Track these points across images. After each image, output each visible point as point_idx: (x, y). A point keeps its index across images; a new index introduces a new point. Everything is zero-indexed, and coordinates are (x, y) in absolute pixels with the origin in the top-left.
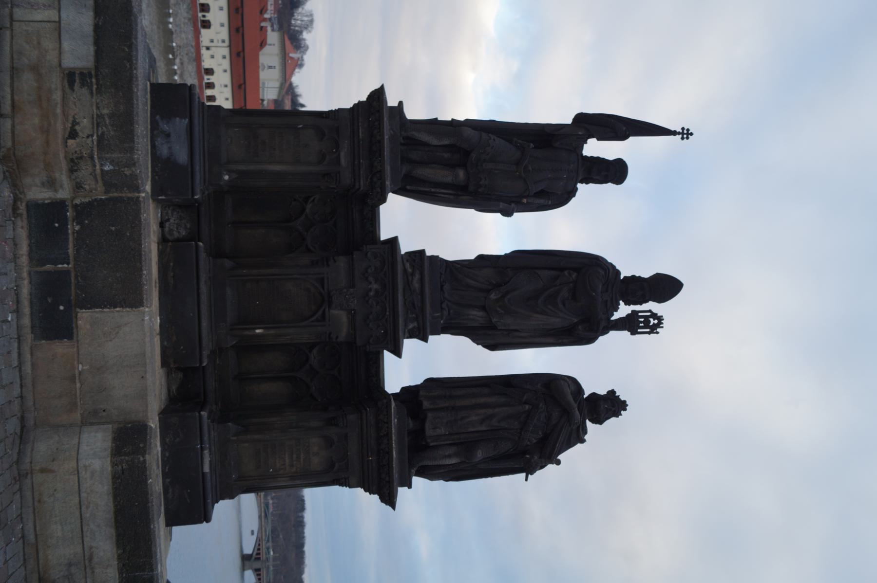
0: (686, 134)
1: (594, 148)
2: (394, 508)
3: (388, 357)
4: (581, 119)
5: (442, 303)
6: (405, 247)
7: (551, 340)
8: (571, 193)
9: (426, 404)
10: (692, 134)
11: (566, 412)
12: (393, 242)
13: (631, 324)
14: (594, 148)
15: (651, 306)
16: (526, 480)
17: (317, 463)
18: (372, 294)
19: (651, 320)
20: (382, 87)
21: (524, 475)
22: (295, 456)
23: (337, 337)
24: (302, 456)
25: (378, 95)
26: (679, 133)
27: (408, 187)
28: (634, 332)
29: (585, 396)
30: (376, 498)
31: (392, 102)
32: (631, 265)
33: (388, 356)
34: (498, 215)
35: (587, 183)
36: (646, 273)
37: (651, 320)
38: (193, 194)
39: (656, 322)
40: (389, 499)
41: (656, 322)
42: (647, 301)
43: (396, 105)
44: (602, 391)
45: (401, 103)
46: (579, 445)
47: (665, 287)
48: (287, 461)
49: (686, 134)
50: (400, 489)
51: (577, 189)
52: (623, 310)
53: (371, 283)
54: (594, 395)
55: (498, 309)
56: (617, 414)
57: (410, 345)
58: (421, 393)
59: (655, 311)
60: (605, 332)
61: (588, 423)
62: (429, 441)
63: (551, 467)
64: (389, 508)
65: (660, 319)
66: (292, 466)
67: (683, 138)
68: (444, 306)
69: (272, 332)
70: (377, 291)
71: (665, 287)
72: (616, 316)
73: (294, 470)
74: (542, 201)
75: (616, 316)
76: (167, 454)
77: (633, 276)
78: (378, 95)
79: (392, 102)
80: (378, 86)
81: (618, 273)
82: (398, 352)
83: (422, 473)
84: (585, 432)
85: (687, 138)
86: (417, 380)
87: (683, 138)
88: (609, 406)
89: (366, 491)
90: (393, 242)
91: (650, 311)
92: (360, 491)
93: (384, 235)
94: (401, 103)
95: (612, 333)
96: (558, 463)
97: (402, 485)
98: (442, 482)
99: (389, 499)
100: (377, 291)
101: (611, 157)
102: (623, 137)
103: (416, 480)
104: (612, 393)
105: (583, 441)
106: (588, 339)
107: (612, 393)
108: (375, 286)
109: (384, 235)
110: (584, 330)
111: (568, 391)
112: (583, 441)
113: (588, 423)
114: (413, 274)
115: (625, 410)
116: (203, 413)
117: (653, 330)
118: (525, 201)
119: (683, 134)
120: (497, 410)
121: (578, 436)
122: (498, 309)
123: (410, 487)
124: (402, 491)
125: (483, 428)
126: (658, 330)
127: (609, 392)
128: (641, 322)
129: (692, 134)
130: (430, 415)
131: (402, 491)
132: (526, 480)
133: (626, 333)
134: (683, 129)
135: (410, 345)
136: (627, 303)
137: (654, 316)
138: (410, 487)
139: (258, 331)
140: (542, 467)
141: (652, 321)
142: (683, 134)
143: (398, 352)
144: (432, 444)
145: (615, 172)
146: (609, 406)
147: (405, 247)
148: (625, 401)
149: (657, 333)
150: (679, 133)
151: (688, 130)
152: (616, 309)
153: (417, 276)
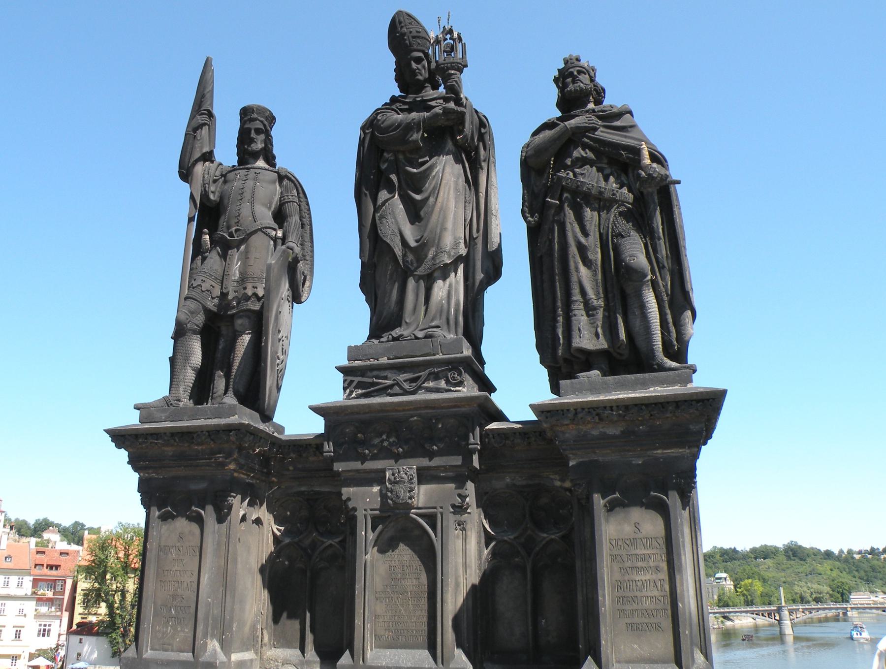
4: (185, 174)
5: (416, 338)
11: (574, 138)
14: (226, 153)
16: (679, 182)
17: (650, 524)
24: (639, 552)
31: (131, 419)
43: (137, 413)
45: (137, 407)
48: (648, 577)
54: (559, 105)
68: (420, 334)
77: (397, 79)
83: (677, 350)
115: (578, 60)
122: (430, 256)
124: (701, 382)
132: (679, 182)
147: (334, 392)
148: (566, 62)
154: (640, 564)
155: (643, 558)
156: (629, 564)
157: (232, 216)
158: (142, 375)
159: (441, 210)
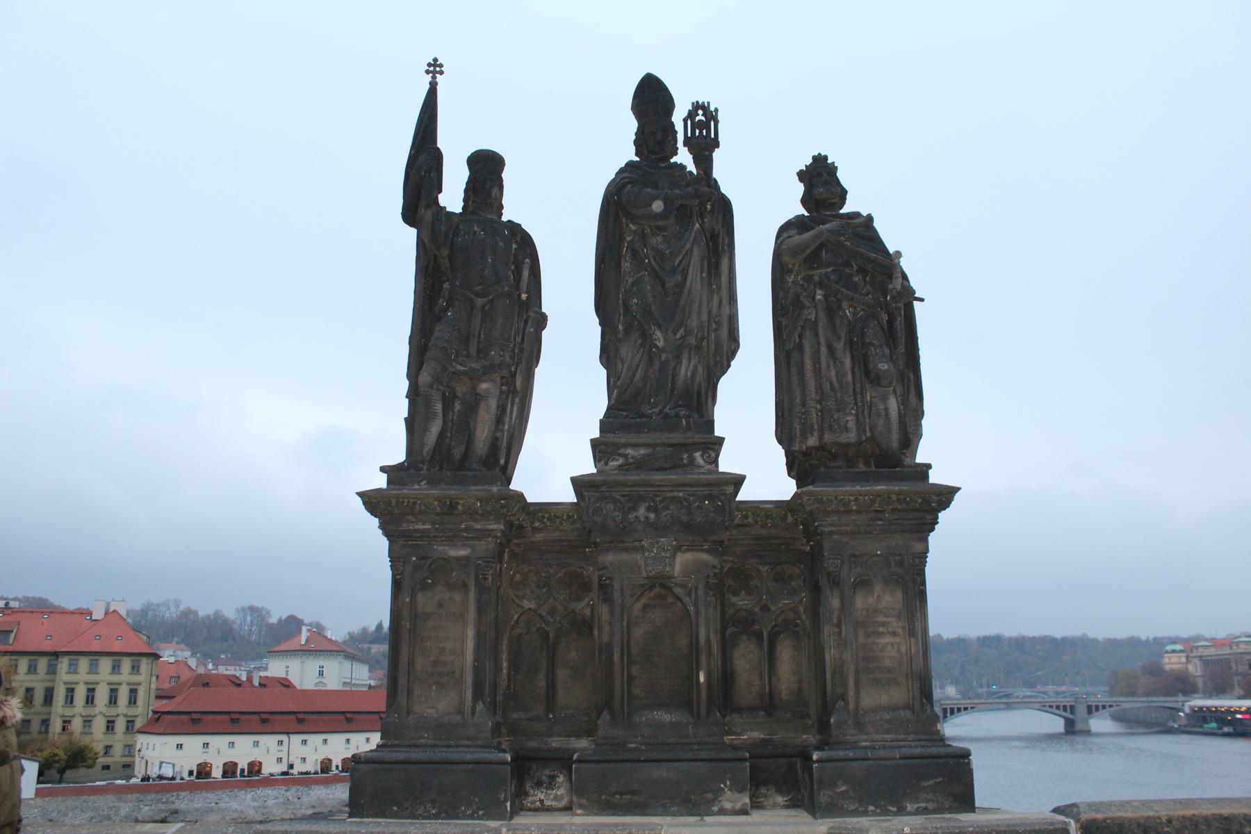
0: (435, 68)
1: (452, 197)
2: (959, 489)
3: (744, 495)
4: (410, 216)
6: (587, 466)
7: (725, 262)
8: (515, 228)
9: (812, 441)
10: (435, 60)
12: (579, 484)
13: (704, 146)
14: (452, 197)
15: (678, 118)
16: (922, 300)
18: (652, 516)
19: (698, 118)
20: (361, 494)
21: (915, 303)
22: (881, 629)
23: (714, 567)
25: (371, 501)
26: (434, 78)
27: (502, 462)
28: (716, 143)
29: (806, 214)
30: (943, 516)
31: (381, 481)
32: (618, 146)
33: (744, 495)
34: (545, 334)
35: (502, 207)
36: (631, 125)
37: (698, 118)
38: (506, 763)
39: (700, 112)
40: (946, 495)
41: (700, 112)
42: (672, 125)
44: (800, 188)
45: (383, 469)
46: (875, 224)
47: (651, 98)
49: (435, 68)
50: (931, 481)
51: (509, 221)
52: (684, 157)
53: (637, 517)
54: (804, 201)
55: (678, 336)
56: (832, 170)
57: (727, 463)
58: (796, 447)
59: (686, 114)
60: (714, 185)
61: (844, 211)
62: (864, 438)
63: (904, 263)
64: (957, 497)
65: (697, 106)
66: (894, 634)
67: (442, 73)
69: (703, 658)
70: (649, 509)
71: (651, 98)
72: (691, 167)
73: (900, 631)
74: (526, 273)
75: (691, 167)
76: (871, 808)
77: (636, 143)
78: (371, 501)
79: (381, 481)
80: (359, 501)
81: (630, 164)
82: (738, 481)
84: (858, 214)
85: (441, 66)
86: (778, 455)
87: (442, 73)
88: (820, 180)
89: (933, 529)
90: (579, 484)
91: (685, 121)
92: (933, 538)
93: (569, 496)
94: (383, 469)
95: (716, 174)
96: (898, 254)
97: (926, 477)
98: (923, 422)
99: (946, 495)
100: (649, 509)
101: (466, 173)
102: (438, 157)
103: (920, 459)
104: (802, 176)
105: (870, 219)
106: (724, 208)
107: (802, 176)
108: (642, 511)
109: (569, 496)
110: (710, 214)
111: (797, 239)
112: (870, 219)
113: (844, 211)
114: (625, 456)
115: (826, 158)
116: (815, 757)
117: (711, 116)
118: (524, 296)
119: (434, 73)
120: (822, 341)
121: (864, 228)
122: (678, 336)
123: (929, 466)
124: (935, 477)
125: (847, 361)
126: (712, 109)
127: (801, 180)
128: (701, 133)
129: (435, 60)
130: (828, 437)
131: (935, 477)
132: (922, 300)
133: (717, 155)
134: (428, 72)
135: (727, 463)
136: (675, 152)
137: (691, 115)
138: (929, 466)
139: (702, 679)
140: (905, 277)
141: (700, 117)
142: (434, 73)
143: (738, 481)
144: (869, 434)
145: (487, 169)
146: (820, 180)
147: (587, 466)
148: (814, 158)
149: (716, 110)
150: (434, 78)
151: (429, 65)
152: (682, 167)
153: (629, 451)
154: (881, 629)
155: (883, 624)
156: (871, 629)
157: (469, 273)
158: (378, 432)
159: (690, 290)
